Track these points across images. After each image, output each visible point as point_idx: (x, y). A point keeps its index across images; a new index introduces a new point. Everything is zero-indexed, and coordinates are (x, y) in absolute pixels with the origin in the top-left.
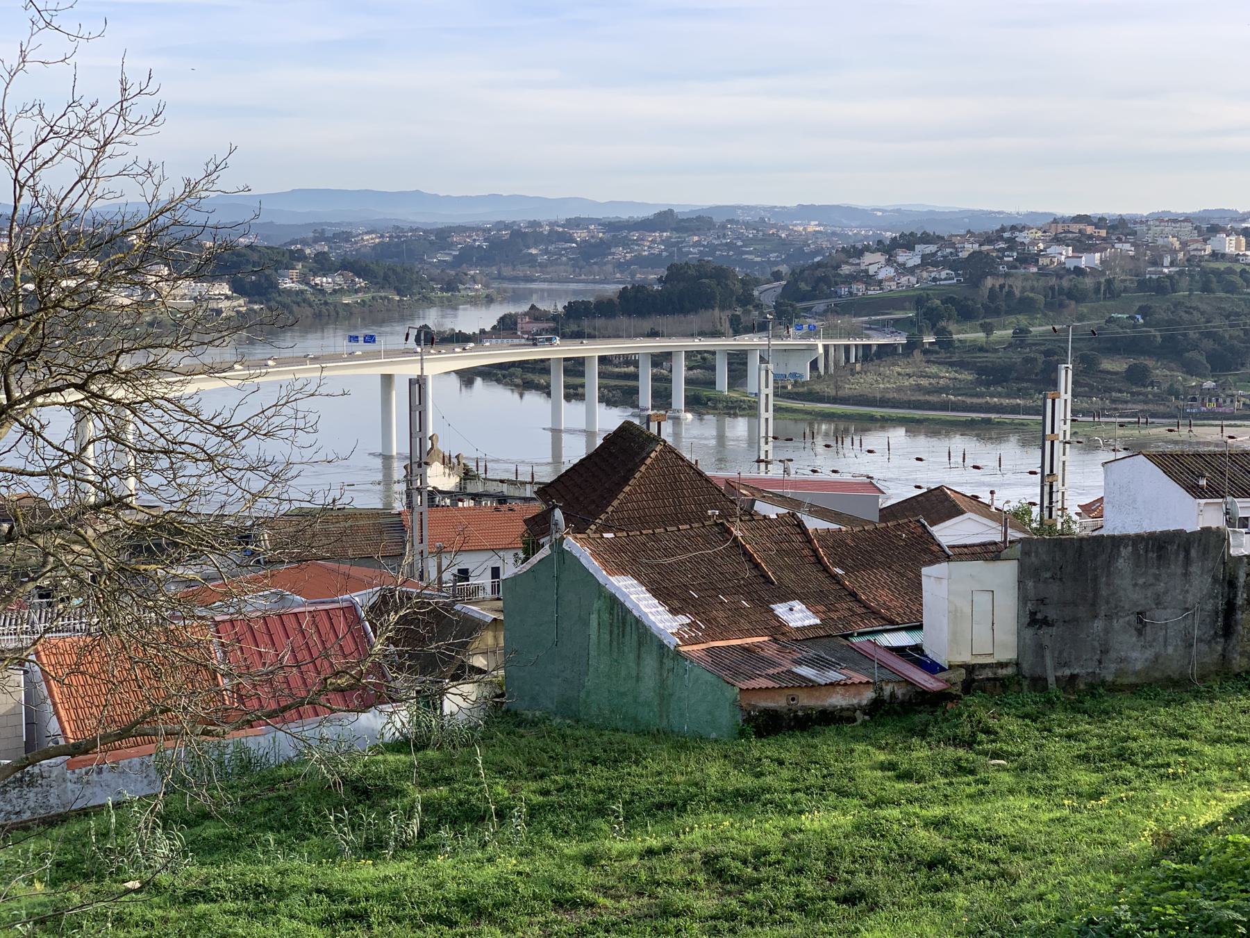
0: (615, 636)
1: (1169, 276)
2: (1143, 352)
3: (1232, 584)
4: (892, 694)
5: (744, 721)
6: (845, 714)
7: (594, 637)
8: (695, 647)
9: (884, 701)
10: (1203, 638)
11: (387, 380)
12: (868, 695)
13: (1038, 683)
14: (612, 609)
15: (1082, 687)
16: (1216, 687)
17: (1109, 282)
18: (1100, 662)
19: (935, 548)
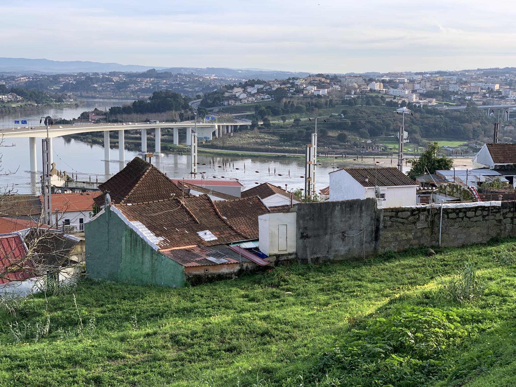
0: (132, 246)
1: (354, 99)
2: (344, 129)
3: (378, 220)
4: (247, 267)
5: (187, 280)
6: (228, 276)
7: (124, 247)
8: (166, 250)
9: (243, 270)
10: (367, 241)
11: (32, 140)
12: (237, 268)
13: (304, 261)
14: (131, 235)
15: (321, 262)
16: (372, 260)
17: (331, 101)
18: (328, 252)
19: (264, 208)
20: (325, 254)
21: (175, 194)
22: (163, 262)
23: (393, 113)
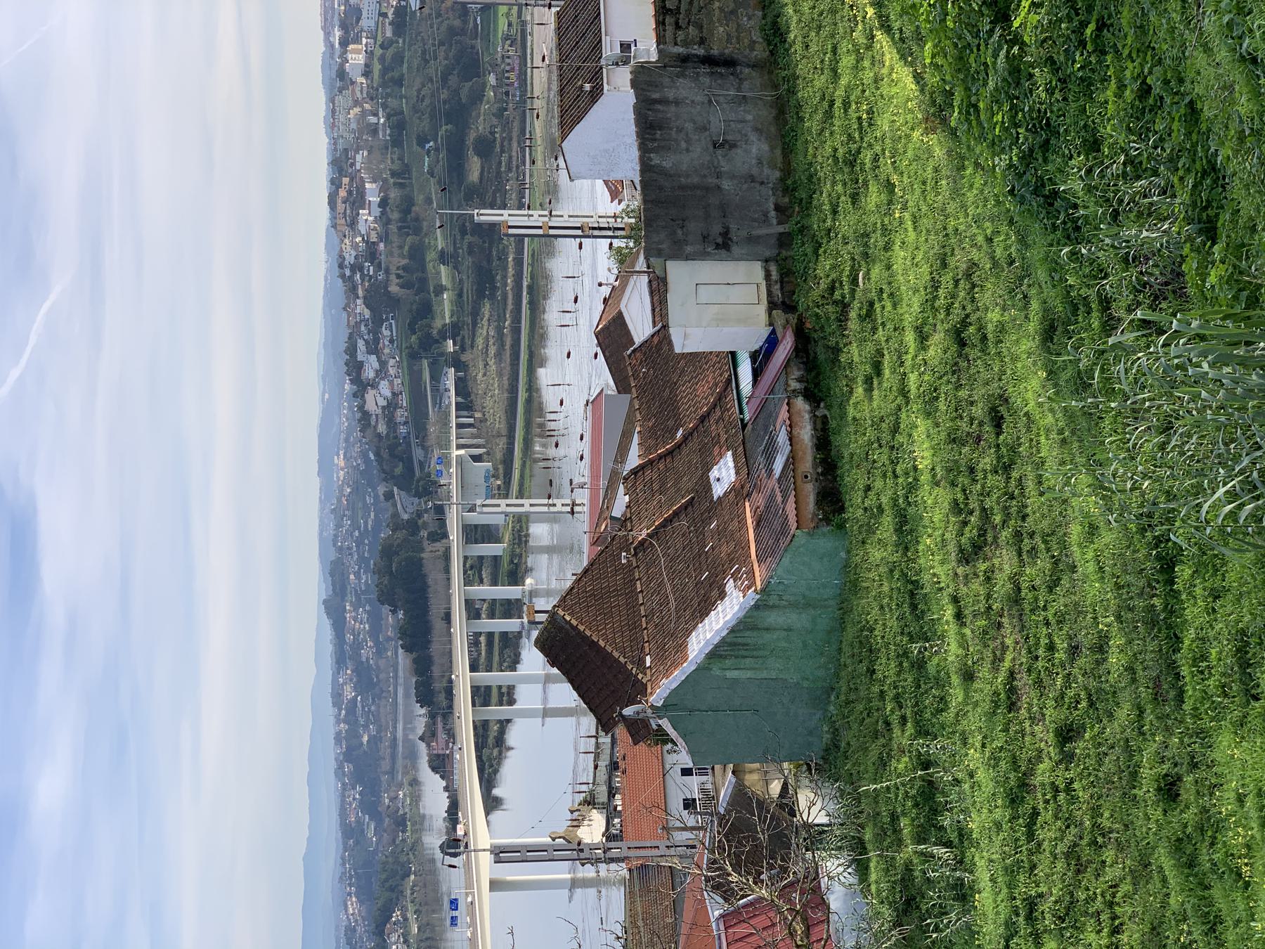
1: (388, 117)
2: (463, 141)
3: (684, 60)
4: (799, 380)
5: (828, 524)
6: (819, 426)
7: (749, 674)
8: (757, 574)
9: (806, 389)
12: (801, 404)
13: (784, 241)
14: (721, 656)
15: (787, 200)
16: (784, 73)
17: (393, 174)
18: (762, 183)
19: (656, 340)
21: (624, 554)
22: (786, 582)
23: (421, 19)
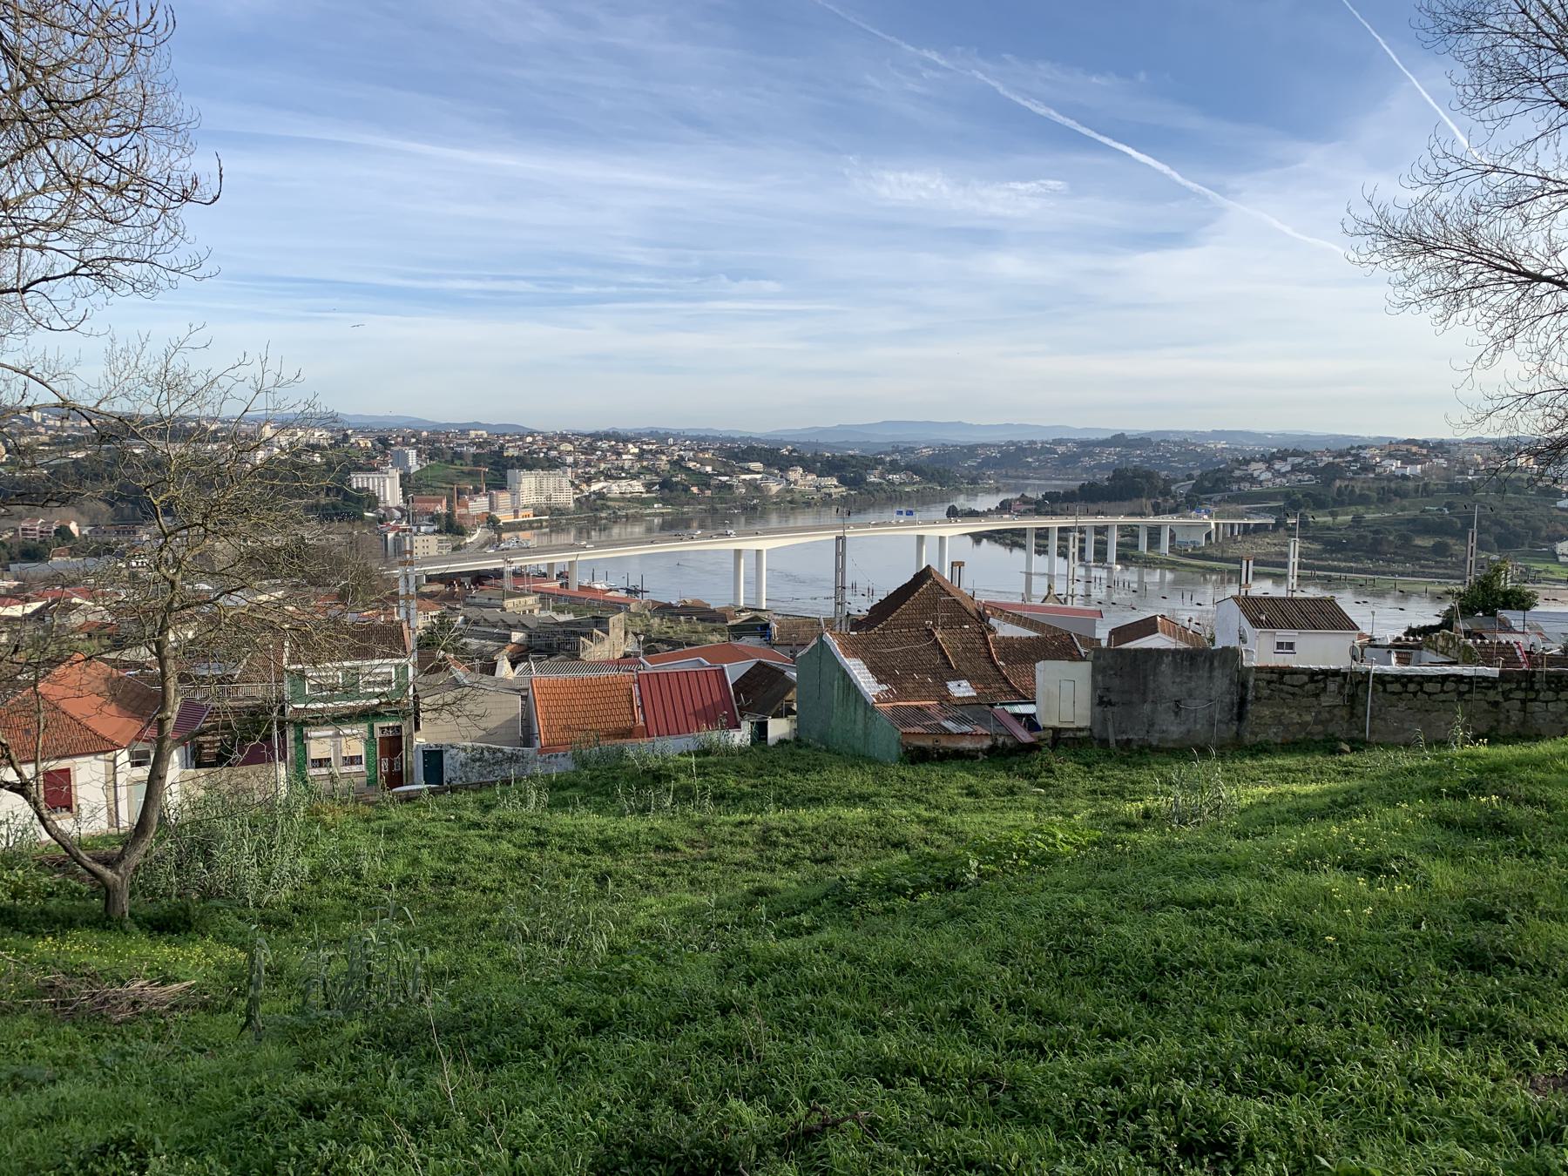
1: (1471, 482)
2: (1446, 534)
3: (1244, 685)
4: (1004, 743)
9: (997, 747)
12: (987, 743)
13: (1104, 743)
16: (1228, 754)
17: (1426, 485)
19: (1075, 653)
20: (1142, 734)
23: (1549, 509)
